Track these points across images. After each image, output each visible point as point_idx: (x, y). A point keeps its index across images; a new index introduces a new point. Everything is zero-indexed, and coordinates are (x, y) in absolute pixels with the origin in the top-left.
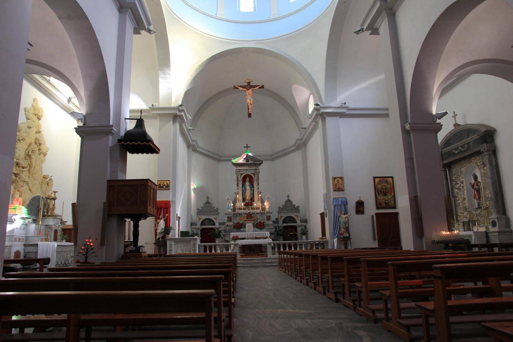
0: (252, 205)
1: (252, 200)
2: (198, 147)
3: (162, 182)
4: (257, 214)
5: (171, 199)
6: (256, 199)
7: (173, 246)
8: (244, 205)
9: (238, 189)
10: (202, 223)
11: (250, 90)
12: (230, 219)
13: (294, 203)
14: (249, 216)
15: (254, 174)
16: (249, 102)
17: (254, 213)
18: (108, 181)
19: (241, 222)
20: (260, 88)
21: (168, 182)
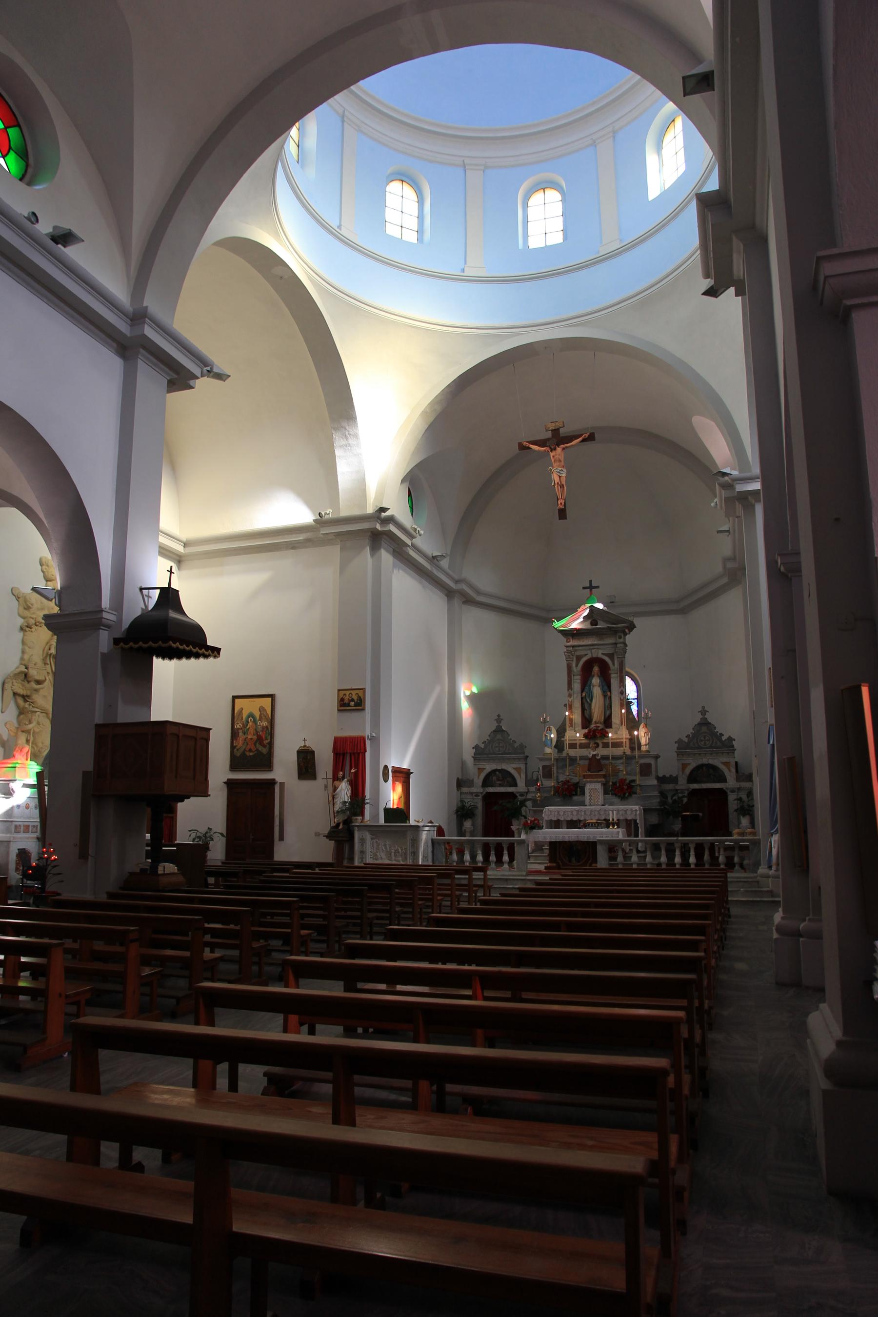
0: (604, 735)
1: (608, 722)
2: (478, 592)
3: (348, 693)
4: (614, 758)
5: (368, 732)
6: (615, 720)
7: (369, 842)
8: (586, 736)
9: (570, 696)
10: (486, 782)
11: (559, 450)
12: (547, 772)
13: (719, 730)
14: (595, 765)
15: (611, 656)
16: (557, 480)
17: (606, 758)
18: (98, 726)
19: (575, 780)
20: (584, 440)
21: (361, 693)
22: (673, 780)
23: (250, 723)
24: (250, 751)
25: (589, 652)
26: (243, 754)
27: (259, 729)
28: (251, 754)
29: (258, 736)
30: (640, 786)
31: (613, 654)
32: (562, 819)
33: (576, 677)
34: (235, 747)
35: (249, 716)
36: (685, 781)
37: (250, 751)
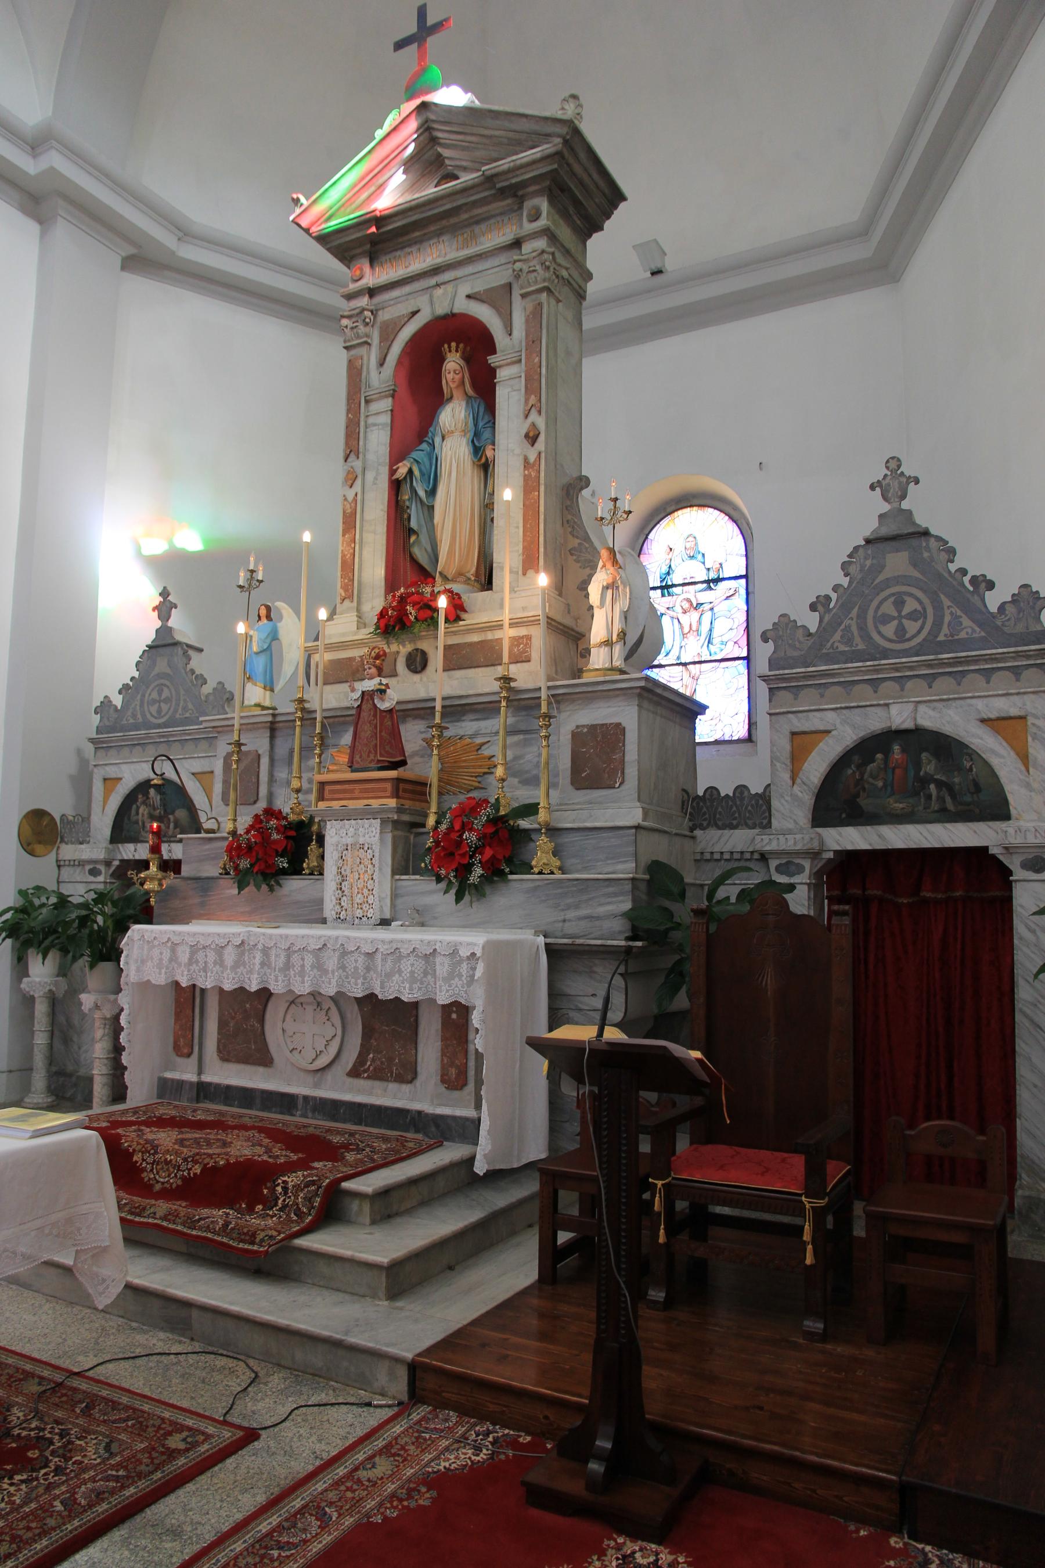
2: (185, 233)
4: (457, 709)
9: (351, 479)
13: (971, 560)
17: (421, 710)
22: (751, 808)
25: (422, 302)
30: (553, 831)
31: (509, 286)
32: (207, 983)
33: (374, 407)
36: (803, 816)
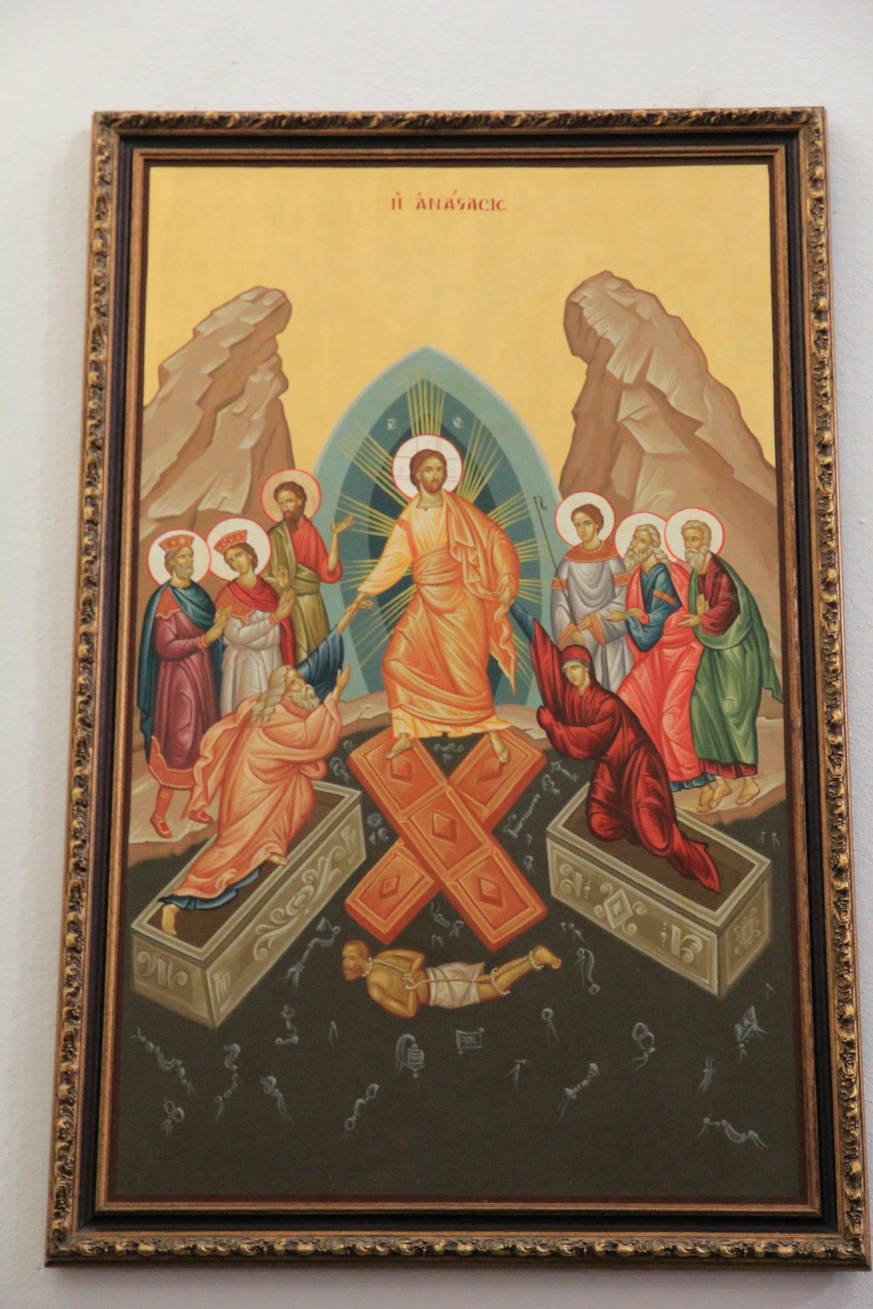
23: (425, 523)
24: (437, 933)
26: (313, 980)
27: (587, 605)
28: (455, 986)
29: (558, 705)
34: (151, 876)
35: (392, 426)
37: (437, 933)
